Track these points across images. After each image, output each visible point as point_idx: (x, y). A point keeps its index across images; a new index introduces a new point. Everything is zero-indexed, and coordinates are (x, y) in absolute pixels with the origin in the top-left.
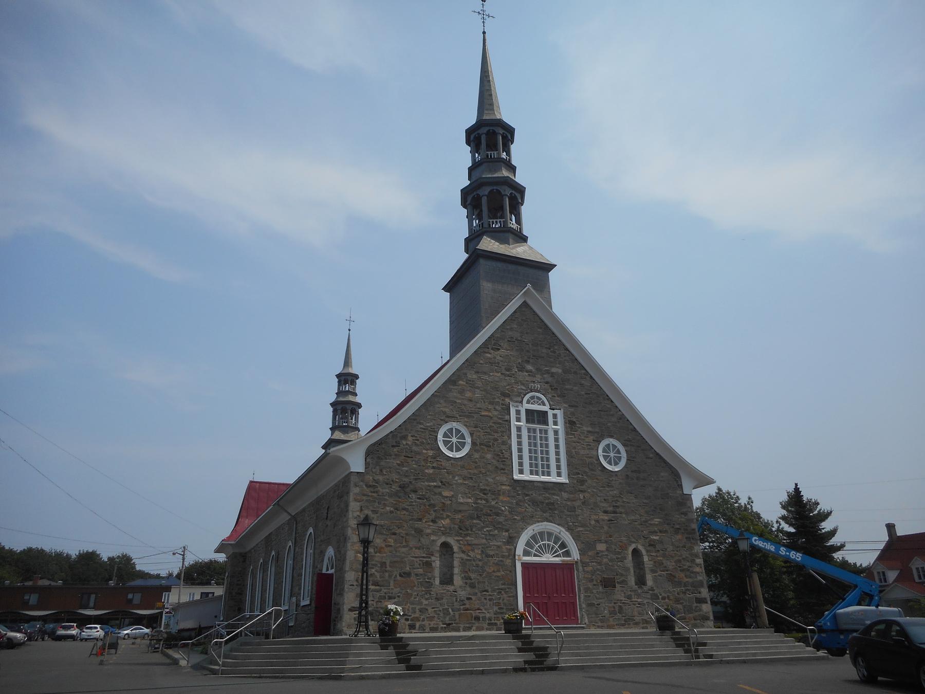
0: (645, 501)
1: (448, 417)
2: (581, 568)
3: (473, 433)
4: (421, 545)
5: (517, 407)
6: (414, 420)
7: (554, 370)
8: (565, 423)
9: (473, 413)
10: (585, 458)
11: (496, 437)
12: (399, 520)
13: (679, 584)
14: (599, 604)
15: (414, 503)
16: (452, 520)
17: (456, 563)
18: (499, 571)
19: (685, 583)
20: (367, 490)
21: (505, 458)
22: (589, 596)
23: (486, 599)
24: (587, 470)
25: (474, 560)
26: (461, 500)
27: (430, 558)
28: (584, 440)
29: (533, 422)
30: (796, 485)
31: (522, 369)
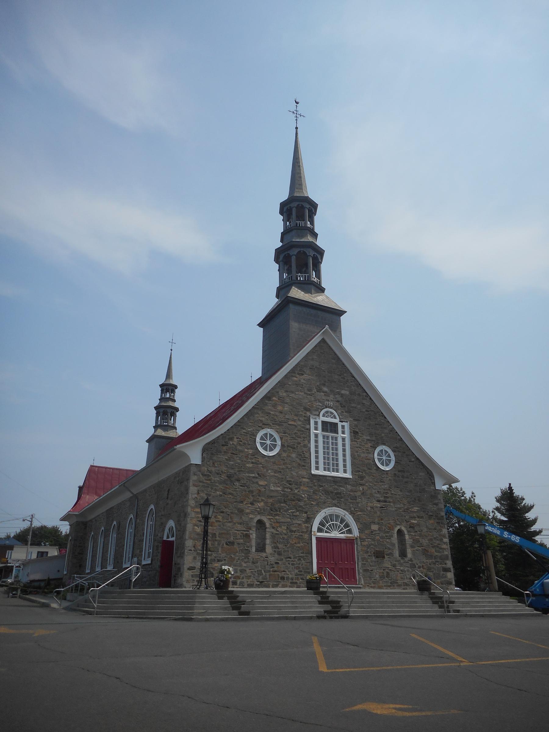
0: (407, 494)
1: (264, 424)
2: (359, 543)
3: (283, 438)
4: (242, 521)
5: (315, 419)
6: (239, 426)
7: (343, 392)
8: (351, 432)
9: (283, 422)
10: (364, 460)
11: (299, 441)
12: (226, 502)
13: (431, 557)
14: (372, 570)
15: (238, 490)
16: (266, 503)
17: (268, 536)
18: (299, 543)
19: (435, 556)
20: (203, 478)
21: (305, 457)
22: (365, 564)
23: (289, 564)
24: (365, 468)
25: (281, 534)
26: (273, 488)
27: (248, 531)
28: (364, 446)
29: (327, 431)
30: (510, 484)
31: (319, 390)
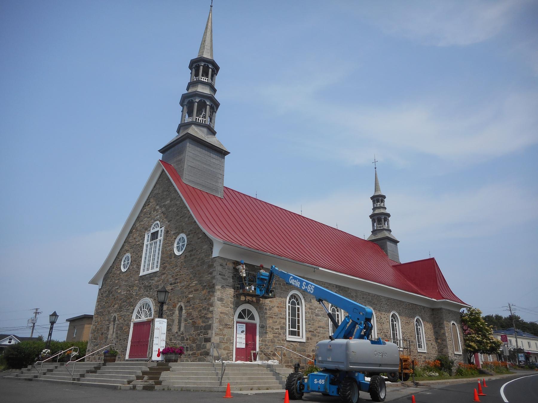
28: (170, 240)
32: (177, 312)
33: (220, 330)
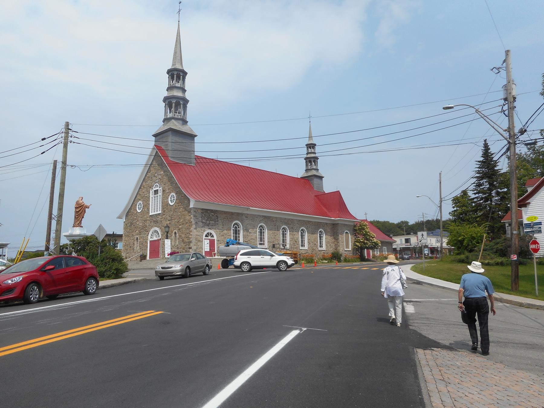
30: (485, 141)
32: (174, 235)
33: (196, 243)
